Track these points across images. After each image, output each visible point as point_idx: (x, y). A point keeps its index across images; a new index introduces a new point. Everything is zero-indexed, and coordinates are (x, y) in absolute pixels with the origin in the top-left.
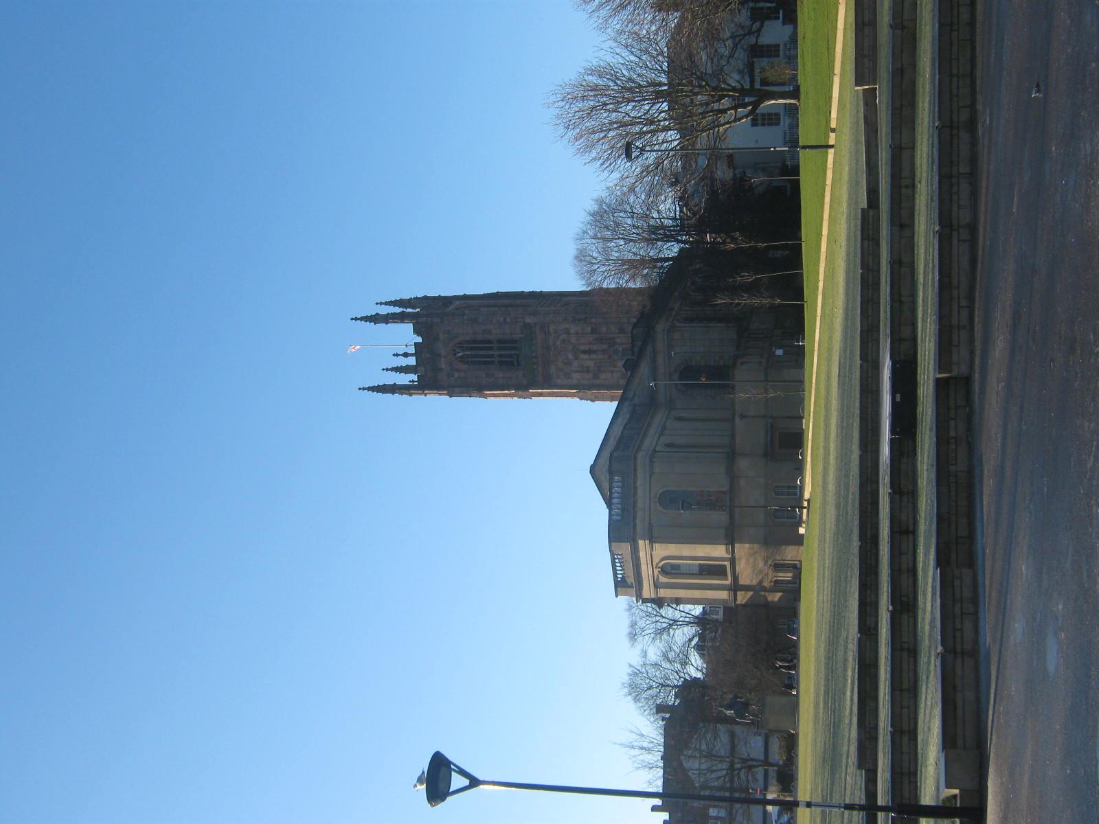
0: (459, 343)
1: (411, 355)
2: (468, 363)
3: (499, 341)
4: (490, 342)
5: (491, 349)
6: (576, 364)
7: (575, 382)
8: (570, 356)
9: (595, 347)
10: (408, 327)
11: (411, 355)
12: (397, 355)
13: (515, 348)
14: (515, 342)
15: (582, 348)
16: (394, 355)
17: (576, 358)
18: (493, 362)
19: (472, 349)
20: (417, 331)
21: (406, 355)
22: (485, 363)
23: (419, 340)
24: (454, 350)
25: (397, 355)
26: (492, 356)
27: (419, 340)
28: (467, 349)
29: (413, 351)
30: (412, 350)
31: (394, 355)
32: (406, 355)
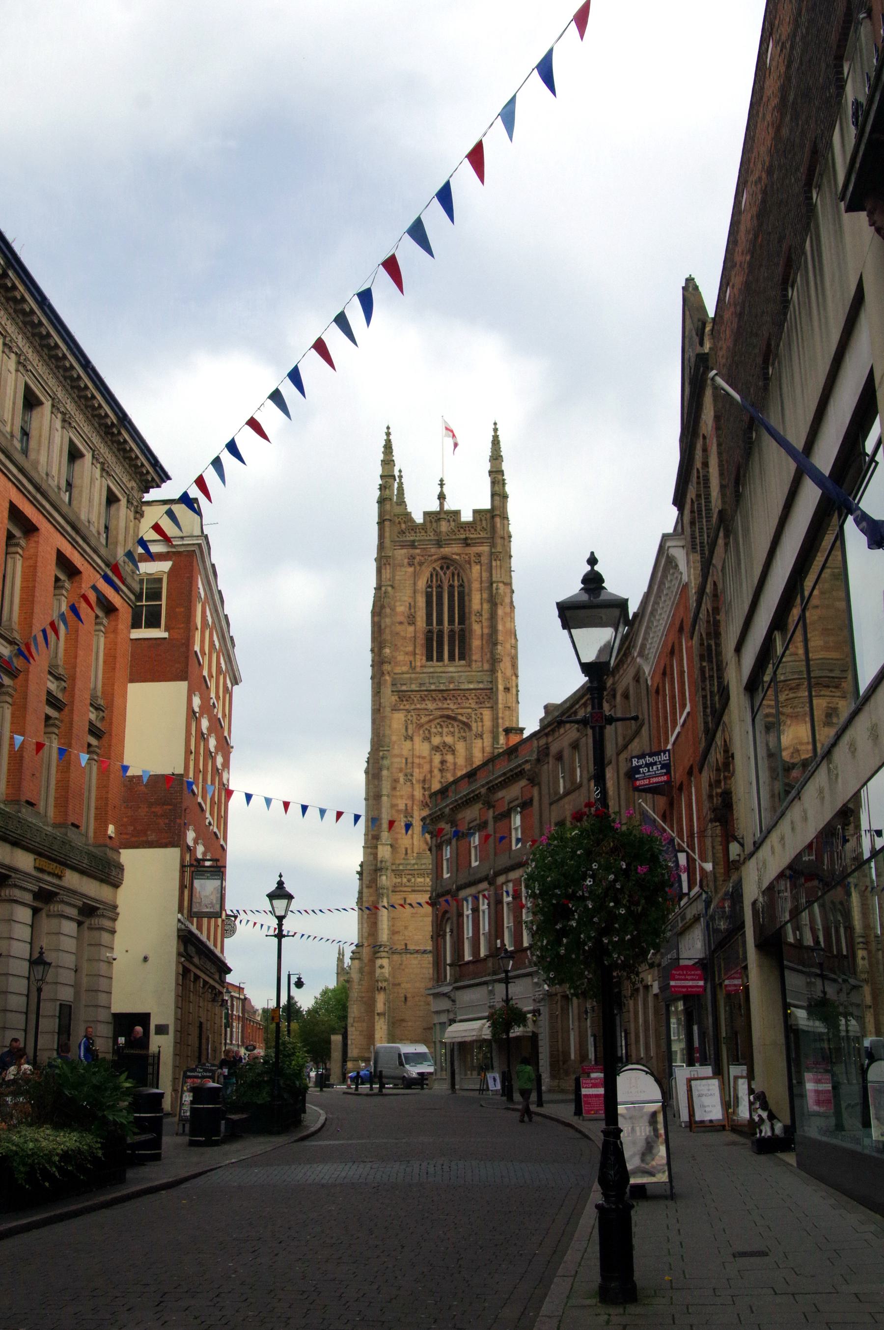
1: (442, 505)
2: (430, 587)
4: (462, 621)
5: (451, 621)
8: (436, 741)
10: (485, 503)
11: (442, 505)
12: (442, 484)
13: (452, 658)
15: (449, 758)
16: (442, 480)
20: (476, 512)
21: (442, 497)
23: (467, 516)
24: (448, 568)
25: (442, 484)
26: (440, 622)
27: (467, 516)
28: (451, 587)
29: (446, 508)
30: (449, 506)
31: (442, 480)
32: (442, 497)
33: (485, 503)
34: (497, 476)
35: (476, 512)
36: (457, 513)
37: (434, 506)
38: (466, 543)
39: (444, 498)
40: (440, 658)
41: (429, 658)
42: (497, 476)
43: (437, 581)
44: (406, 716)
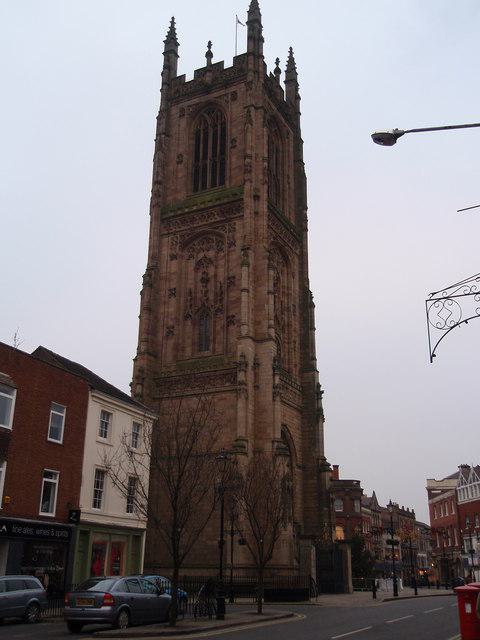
1: (209, 61)
3: (223, 163)
4: (223, 152)
6: (192, 264)
8: (201, 255)
12: (210, 45)
13: (214, 185)
14: (222, 183)
16: (210, 42)
17: (199, 264)
18: (197, 158)
19: (215, 134)
21: (209, 55)
25: (210, 45)
27: (229, 64)
30: (214, 61)
31: (210, 42)
32: (209, 55)
35: (236, 59)
36: (221, 63)
37: (203, 64)
38: (226, 85)
40: (204, 186)
41: (196, 189)
44: (172, 239)
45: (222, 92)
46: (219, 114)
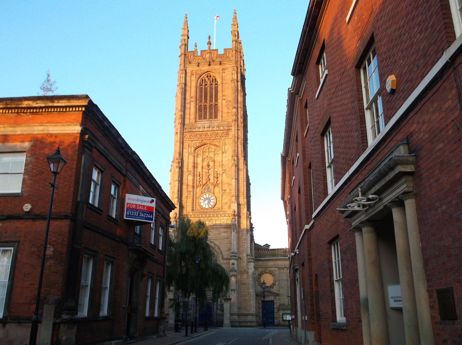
0: (215, 79)
1: (209, 48)
4: (216, 100)
5: (211, 101)
7: (185, 158)
9: (211, 171)
10: (230, 45)
11: (209, 48)
12: (209, 38)
14: (216, 117)
15: (211, 164)
16: (209, 36)
18: (201, 101)
19: (211, 89)
21: (210, 43)
22: (201, 97)
25: (209, 38)
31: (209, 36)
33: (230, 45)
34: (236, 35)
36: (217, 50)
37: (206, 47)
39: (211, 44)
42: (236, 35)
43: (205, 82)
45: (217, 67)
46: (214, 78)
